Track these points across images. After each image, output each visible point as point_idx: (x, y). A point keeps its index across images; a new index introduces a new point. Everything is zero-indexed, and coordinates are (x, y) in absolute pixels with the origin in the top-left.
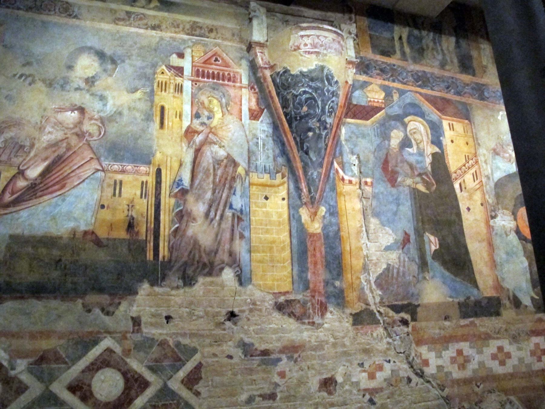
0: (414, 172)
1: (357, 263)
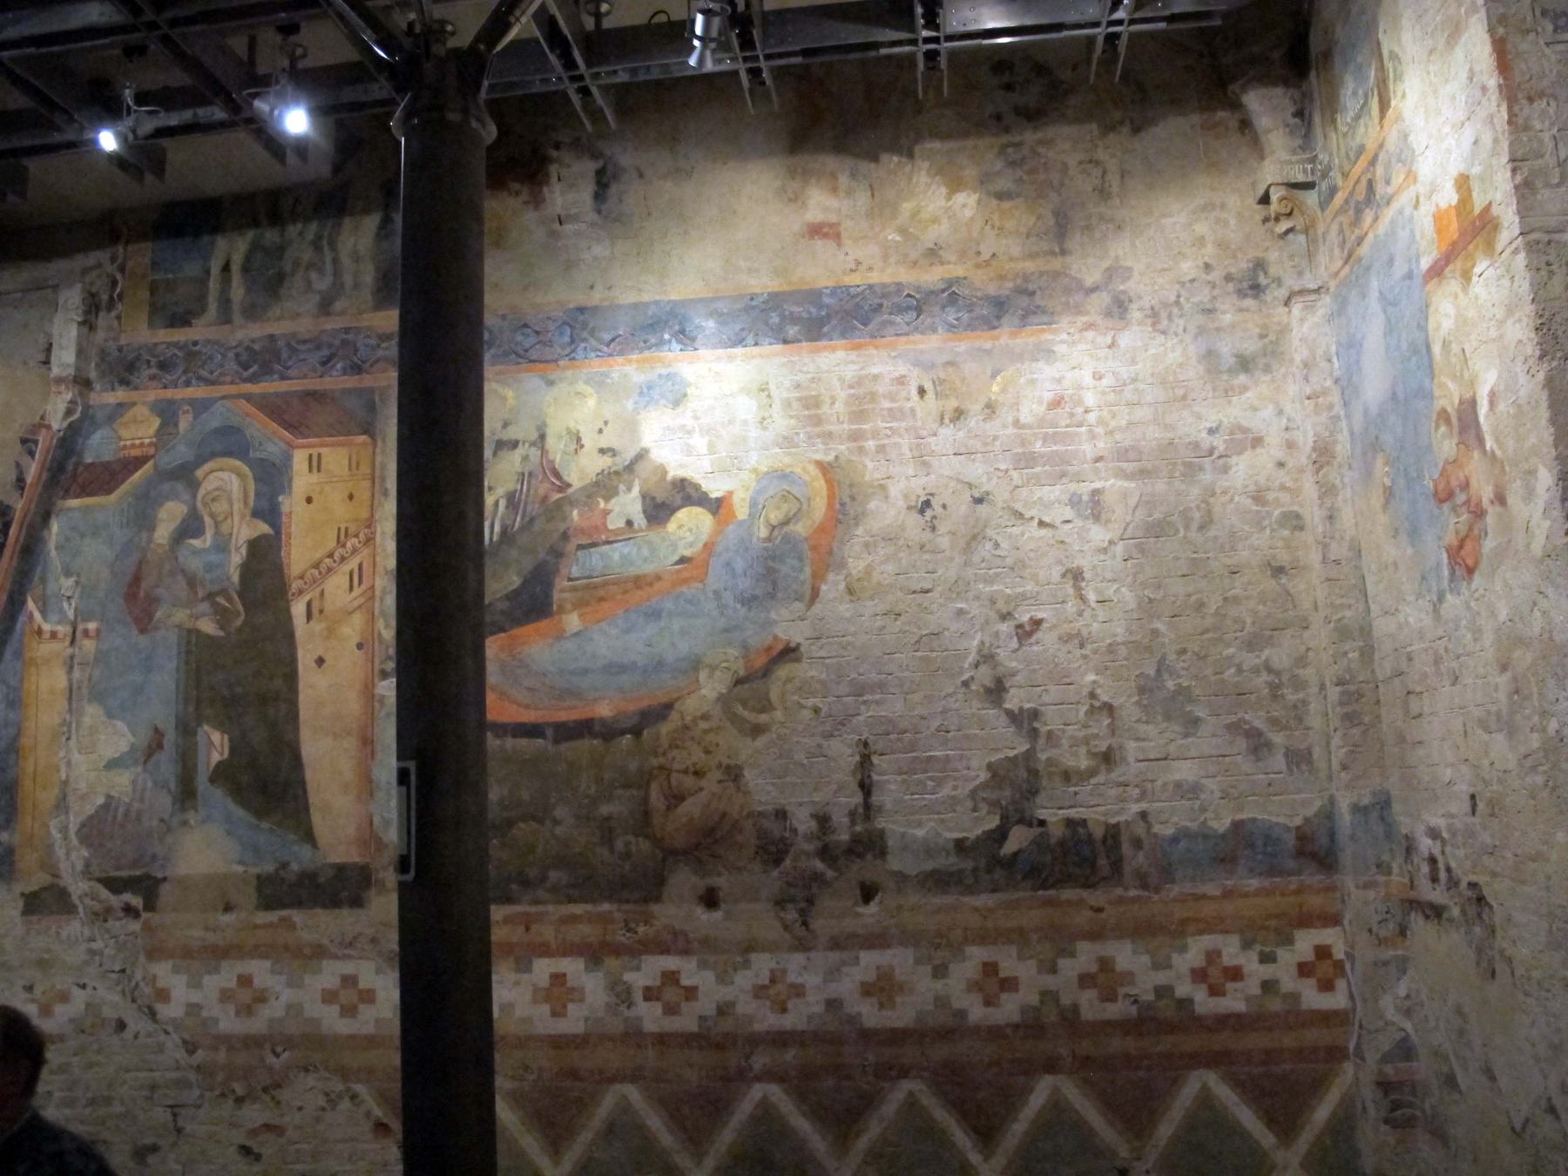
0: (196, 593)
1: (48, 797)
